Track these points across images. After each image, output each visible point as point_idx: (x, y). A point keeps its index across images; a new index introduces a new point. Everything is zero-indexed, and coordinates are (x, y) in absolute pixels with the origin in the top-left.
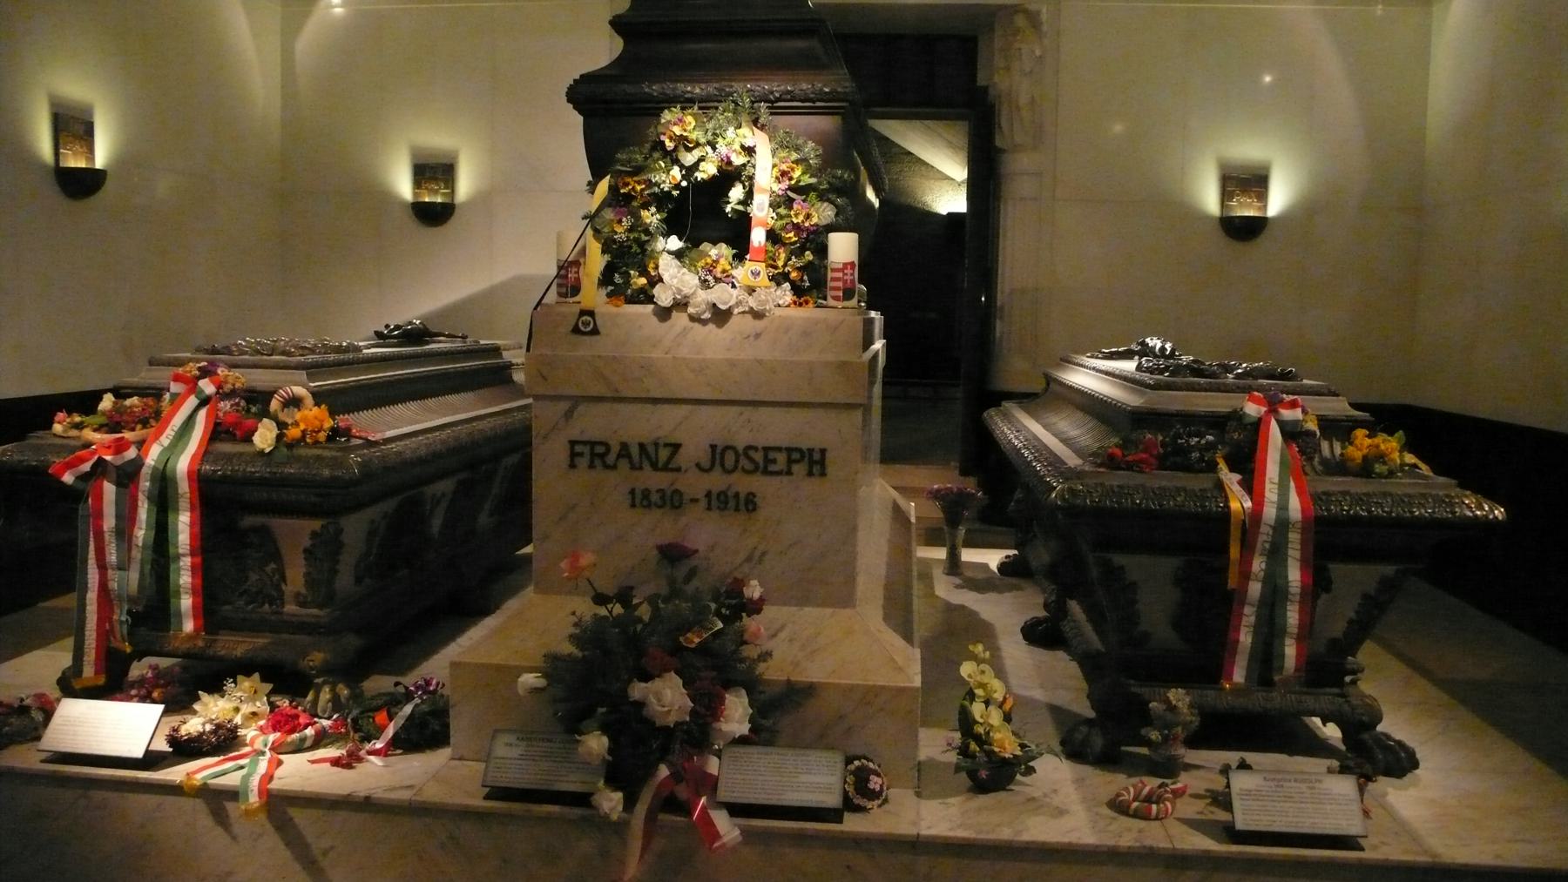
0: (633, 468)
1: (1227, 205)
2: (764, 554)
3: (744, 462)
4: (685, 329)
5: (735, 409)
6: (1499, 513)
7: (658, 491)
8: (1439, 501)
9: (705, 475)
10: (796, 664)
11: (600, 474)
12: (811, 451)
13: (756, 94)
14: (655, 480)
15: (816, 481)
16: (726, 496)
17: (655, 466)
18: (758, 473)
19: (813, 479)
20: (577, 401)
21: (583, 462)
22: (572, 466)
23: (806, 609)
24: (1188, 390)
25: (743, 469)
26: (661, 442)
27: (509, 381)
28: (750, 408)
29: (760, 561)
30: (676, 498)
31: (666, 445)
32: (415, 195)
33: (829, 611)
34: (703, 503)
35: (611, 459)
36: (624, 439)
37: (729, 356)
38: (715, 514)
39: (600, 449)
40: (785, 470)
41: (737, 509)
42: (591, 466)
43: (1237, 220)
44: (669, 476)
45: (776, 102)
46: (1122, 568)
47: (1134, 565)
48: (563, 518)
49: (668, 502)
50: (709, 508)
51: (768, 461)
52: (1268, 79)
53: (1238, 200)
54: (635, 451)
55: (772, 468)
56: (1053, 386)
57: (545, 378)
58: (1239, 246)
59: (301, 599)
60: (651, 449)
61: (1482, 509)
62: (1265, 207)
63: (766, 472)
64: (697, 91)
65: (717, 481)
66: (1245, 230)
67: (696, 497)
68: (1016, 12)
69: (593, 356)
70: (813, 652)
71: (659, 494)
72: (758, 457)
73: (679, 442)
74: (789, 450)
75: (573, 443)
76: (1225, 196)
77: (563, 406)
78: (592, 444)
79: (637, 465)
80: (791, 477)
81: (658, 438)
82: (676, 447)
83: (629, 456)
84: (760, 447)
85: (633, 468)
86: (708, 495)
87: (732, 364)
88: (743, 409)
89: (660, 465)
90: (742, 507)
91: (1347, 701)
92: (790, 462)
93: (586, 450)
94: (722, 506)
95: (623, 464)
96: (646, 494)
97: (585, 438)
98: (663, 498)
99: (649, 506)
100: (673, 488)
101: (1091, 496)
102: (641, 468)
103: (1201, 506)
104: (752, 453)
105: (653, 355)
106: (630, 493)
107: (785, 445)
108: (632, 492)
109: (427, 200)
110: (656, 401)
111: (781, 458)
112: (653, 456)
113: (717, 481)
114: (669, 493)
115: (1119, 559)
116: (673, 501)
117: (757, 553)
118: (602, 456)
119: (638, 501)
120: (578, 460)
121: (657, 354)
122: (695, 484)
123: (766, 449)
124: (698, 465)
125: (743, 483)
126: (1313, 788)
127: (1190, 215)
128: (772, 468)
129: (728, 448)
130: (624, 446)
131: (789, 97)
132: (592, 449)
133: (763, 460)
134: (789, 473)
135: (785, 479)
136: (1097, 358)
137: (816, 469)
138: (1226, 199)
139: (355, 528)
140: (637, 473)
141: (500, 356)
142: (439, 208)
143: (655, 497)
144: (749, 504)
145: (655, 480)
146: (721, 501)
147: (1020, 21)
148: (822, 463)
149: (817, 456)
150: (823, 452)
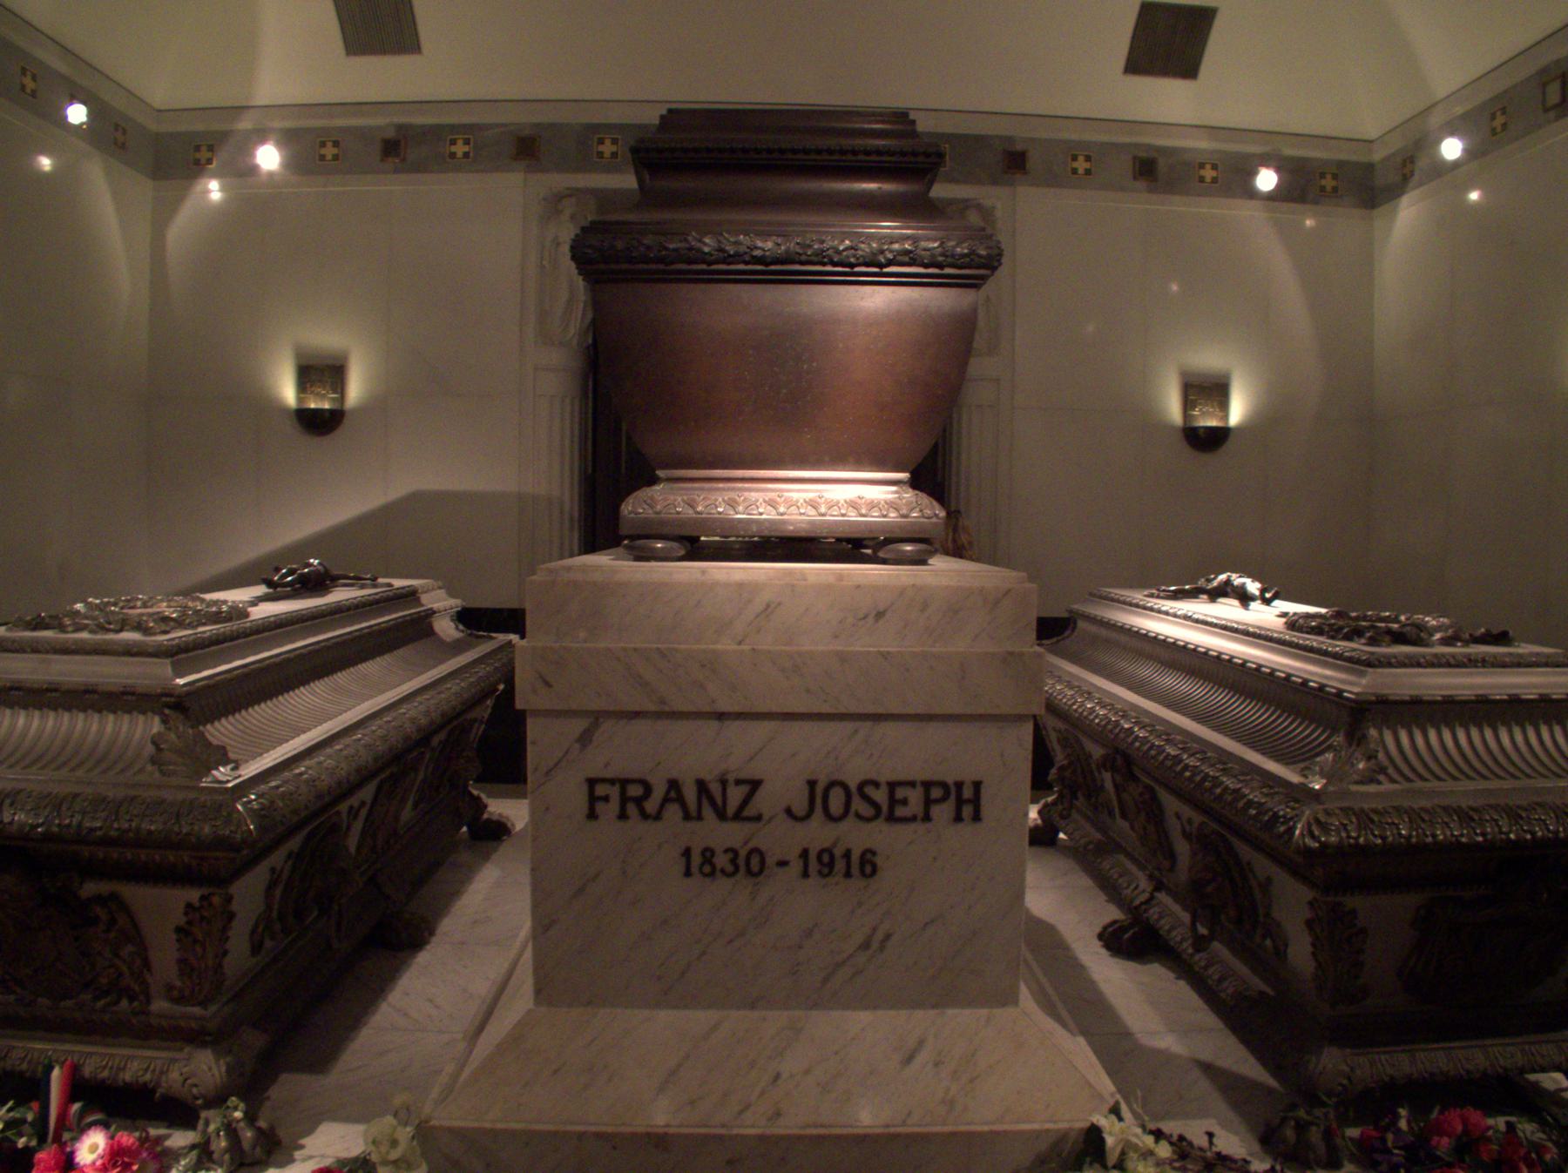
0: (687, 817)
1: (1190, 415)
2: (888, 937)
3: (858, 805)
4: (768, 606)
5: (849, 726)
7: (726, 851)
9: (798, 826)
10: (950, 1103)
11: (635, 825)
12: (959, 785)
13: (860, 253)
14: (721, 835)
15: (967, 829)
16: (832, 857)
17: (721, 815)
18: (881, 820)
19: (960, 826)
20: (598, 717)
22: (592, 815)
23: (950, 1012)
24: (1412, 666)
25: (859, 816)
26: (731, 778)
27: (429, 632)
28: (869, 724)
29: (882, 947)
30: (755, 861)
31: (738, 782)
32: (299, 400)
33: (984, 1012)
34: (796, 867)
35: (651, 806)
36: (674, 774)
37: (839, 646)
38: (814, 880)
39: (635, 791)
40: (921, 815)
41: (848, 874)
42: (623, 816)
43: (1202, 430)
44: (748, 828)
45: (890, 263)
46: (1354, 912)
48: (581, 891)
49: (742, 868)
50: (805, 874)
51: (893, 802)
53: (1200, 410)
54: (690, 794)
57: (548, 684)
58: (1205, 457)
60: (715, 788)
62: (1226, 417)
63: (891, 818)
64: (769, 245)
65: (818, 834)
66: (1215, 439)
67: (787, 858)
68: (967, 208)
69: (625, 650)
70: (972, 1081)
71: (730, 855)
72: (880, 796)
74: (927, 785)
75: (592, 783)
76: (1187, 405)
77: (578, 726)
78: (624, 783)
80: (928, 825)
82: (755, 785)
85: (687, 817)
86: (805, 854)
87: (843, 657)
88: (858, 724)
89: (731, 810)
90: (855, 870)
92: (928, 802)
93: (614, 792)
94: (826, 871)
95: (673, 811)
96: (708, 854)
97: (609, 774)
98: (734, 861)
99: (712, 874)
100: (751, 845)
101: (1346, 829)
102: (700, 817)
103: (1483, 834)
104: (869, 790)
105: (719, 647)
106: (683, 855)
107: (921, 775)
108: (687, 853)
109: (313, 406)
110: (721, 716)
111: (915, 797)
112: (719, 801)
113: (818, 834)
114: (743, 853)
115: (1354, 901)
117: (880, 935)
118: (639, 801)
119: (694, 869)
120: (600, 806)
121: (726, 645)
122: (781, 839)
123: (892, 786)
124: (789, 812)
125: (856, 836)
127: (1151, 424)
128: (900, 811)
129: (832, 784)
130: (674, 784)
131: (906, 259)
134: (927, 818)
135: (919, 828)
136: (1158, 597)
137: (967, 811)
138: (1189, 407)
141: (418, 602)
142: (327, 415)
143: (722, 861)
144: (868, 865)
145: (721, 835)
146: (825, 863)
148: (976, 801)
149: (967, 793)
150: (977, 785)
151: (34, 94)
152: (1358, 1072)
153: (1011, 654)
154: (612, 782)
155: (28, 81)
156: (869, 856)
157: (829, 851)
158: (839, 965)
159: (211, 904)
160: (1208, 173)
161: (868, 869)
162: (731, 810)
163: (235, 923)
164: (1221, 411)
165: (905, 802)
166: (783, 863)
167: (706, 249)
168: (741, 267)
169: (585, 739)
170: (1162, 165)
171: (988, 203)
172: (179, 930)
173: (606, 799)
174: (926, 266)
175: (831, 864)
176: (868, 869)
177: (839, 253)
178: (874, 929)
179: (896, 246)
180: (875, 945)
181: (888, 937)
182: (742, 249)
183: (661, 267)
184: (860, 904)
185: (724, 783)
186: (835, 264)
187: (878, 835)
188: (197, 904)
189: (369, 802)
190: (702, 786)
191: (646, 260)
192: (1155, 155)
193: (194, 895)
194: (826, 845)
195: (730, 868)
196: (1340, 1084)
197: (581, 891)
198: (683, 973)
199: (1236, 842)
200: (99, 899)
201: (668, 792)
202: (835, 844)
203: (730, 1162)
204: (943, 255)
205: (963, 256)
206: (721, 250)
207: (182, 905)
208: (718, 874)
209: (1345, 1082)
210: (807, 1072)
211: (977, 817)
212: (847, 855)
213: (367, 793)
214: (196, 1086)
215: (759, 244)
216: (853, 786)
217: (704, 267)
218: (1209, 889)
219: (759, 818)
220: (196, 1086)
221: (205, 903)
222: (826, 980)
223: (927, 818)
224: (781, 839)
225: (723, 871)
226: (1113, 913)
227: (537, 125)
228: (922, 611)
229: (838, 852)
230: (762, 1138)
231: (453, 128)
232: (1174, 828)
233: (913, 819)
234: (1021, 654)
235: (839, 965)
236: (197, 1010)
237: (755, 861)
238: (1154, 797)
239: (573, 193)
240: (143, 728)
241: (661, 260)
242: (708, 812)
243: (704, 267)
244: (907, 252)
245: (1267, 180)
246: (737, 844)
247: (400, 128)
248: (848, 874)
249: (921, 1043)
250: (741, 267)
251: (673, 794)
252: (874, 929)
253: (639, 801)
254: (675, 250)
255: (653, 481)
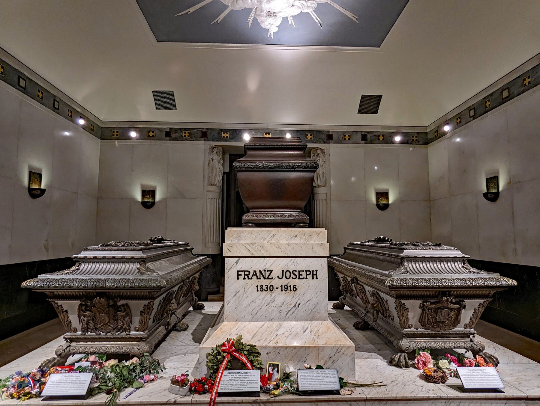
0: (257, 278)
2: (299, 304)
3: (292, 275)
6: (515, 283)
7: (265, 286)
8: (497, 279)
12: (313, 271)
14: (263, 282)
17: (265, 278)
21: (241, 277)
22: (238, 279)
23: (313, 322)
28: (294, 258)
29: (298, 307)
30: (271, 287)
31: (268, 271)
32: (142, 199)
33: (321, 322)
35: (250, 276)
36: (254, 270)
39: (247, 273)
40: (305, 277)
42: (244, 279)
47: (407, 302)
48: (236, 295)
50: (282, 291)
51: (299, 275)
52: (376, 168)
54: (258, 273)
55: (301, 277)
56: (347, 251)
59: (137, 328)
61: (509, 281)
62: (388, 201)
63: (299, 278)
64: (272, 165)
65: (284, 281)
68: (317, 149)
71: (266, 286)
72: (297, 273)
73: (272, 270)
74: (306, 271)
75: (238, 271)
78: (245, 271)
79: (259, 278)
81: (266, 269)
82: (271, 271)
83: (256, 275)
84: (297, 270)
85: (257, 278)
86: (282, 286)
89: (266, 277)
90: (292, 289)
91: (473, 343)
92: (307, 275)
95: (255, 277)
96: (262, 287)
98: (267, 288)
99: (262, 291)
100: (271, 284)
102: (260, 279)
104: (294, 272)
110: (264, 257)
111: (304, 274)
113: (284, 281)
114: (269, 286)
115: (403, 301)
116: (270, 288)
117: (297, 304)
118: (248, 275)
119: (259, 290)
123: (299, 271)
124: (278, 277)
125: (292, 282)
126: (484, 372)
128: (301, 277)
129: (287, 271)
130: (255, 271)
132: (244, 273)
133: (298, 275)
134: (306, 278)
137: (315, 277)
139: (157, 302)
140: (259, 280)
143: (265, 288)
146: (286, 288)
147: (319, 151)
148: (316, 275)
149: (315, 273)
150: (317, 271)
151: (71, 116)
152: (412, 345)
153: (322, 244)
154: (242, 271)
155: (70, 113)
156: (295, 286)
157: (287, 285)
158: (289, 311)
159: (150, 304)
160: (381, 138)
161: (295, 289)
162: (266, 277)
163: (154, 310)
164: (386, 199)
165: (302, 275)
166: (277, 288)
167: (260, 166)
168: (267, 169)
169: (237, 262)
170: (368, 135)
171: (323, 148)
172: (141, 312)
173: (241, 275)
174: (303, 168)
175: (287, 288)
176: (295, 289)
177: (286, 166)
178: (297, 303)
179: (297, 165)
180: (297, 306)
181: (299, 304)
182: (267, 165)
183: (251, 169)
184: (293, 297)
185: (265, 271)
186: (285, 168)
187: (297, 282)
188: (147, 305)
189: (177, 290)
190: (260, 272)
191: (248, 168)
192: (366, 134)
193: (146, 302)
194: (286, 284)
195: (266, 290)
196: (407, 347)
197: (236, 295)
198: (257, 313)
199: (381, 294)
200: (123, 305)
201: (254, 273)
202: (288, 284)
203: (267, 353)
204: (307, 166)
205: (311, 166)
206: (263, 166)
207: (143, 305)
208: (264, 290)
209: (408, 347)
210: (283, 334)
211: (317, 278)
212: (290, 286)
213: (176, 288)
214: (141, 351)
215: (271, 165)
216: (291, 272)
217: (259, 169)
218: (375, 306)
219: (272, 279)
220: (141, 351)
221: (149, 304)
222: (287, 314)
223: (306, 278)
224: (277, 283)
225: (265, 290)
226: (355, 320)
227: (207, 129)
228: (304, 235)
229: (288, 286)
230: (274, 347)
231: (185, 129)
232: (368, 294)
233: (303, 278)
234: (324, 244)
235: (289, 311)
236: (142, 333)
237: (271, 287)
238: (363, 288)
239: (216, 147)
240: (135, 266)
241: (251, 168)
242: (262, 277)
243: (259, 169)
244: (299, 166)
245: (398, 139)
246: (267, 284)
247: (170, 128)
248: (291, 291)
249: (307, 328)
250: (267, 169)
251: (254, 274)
252: (297, 303)
253: (248, 275)
254: (254, 166)
255: (250, 212)
